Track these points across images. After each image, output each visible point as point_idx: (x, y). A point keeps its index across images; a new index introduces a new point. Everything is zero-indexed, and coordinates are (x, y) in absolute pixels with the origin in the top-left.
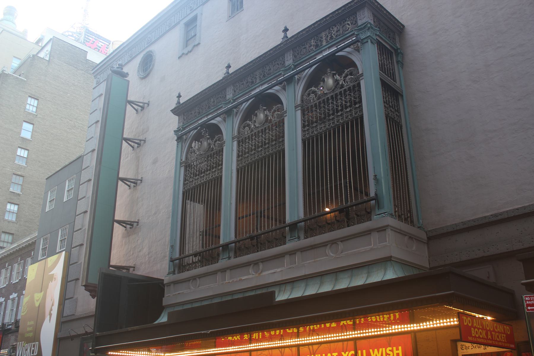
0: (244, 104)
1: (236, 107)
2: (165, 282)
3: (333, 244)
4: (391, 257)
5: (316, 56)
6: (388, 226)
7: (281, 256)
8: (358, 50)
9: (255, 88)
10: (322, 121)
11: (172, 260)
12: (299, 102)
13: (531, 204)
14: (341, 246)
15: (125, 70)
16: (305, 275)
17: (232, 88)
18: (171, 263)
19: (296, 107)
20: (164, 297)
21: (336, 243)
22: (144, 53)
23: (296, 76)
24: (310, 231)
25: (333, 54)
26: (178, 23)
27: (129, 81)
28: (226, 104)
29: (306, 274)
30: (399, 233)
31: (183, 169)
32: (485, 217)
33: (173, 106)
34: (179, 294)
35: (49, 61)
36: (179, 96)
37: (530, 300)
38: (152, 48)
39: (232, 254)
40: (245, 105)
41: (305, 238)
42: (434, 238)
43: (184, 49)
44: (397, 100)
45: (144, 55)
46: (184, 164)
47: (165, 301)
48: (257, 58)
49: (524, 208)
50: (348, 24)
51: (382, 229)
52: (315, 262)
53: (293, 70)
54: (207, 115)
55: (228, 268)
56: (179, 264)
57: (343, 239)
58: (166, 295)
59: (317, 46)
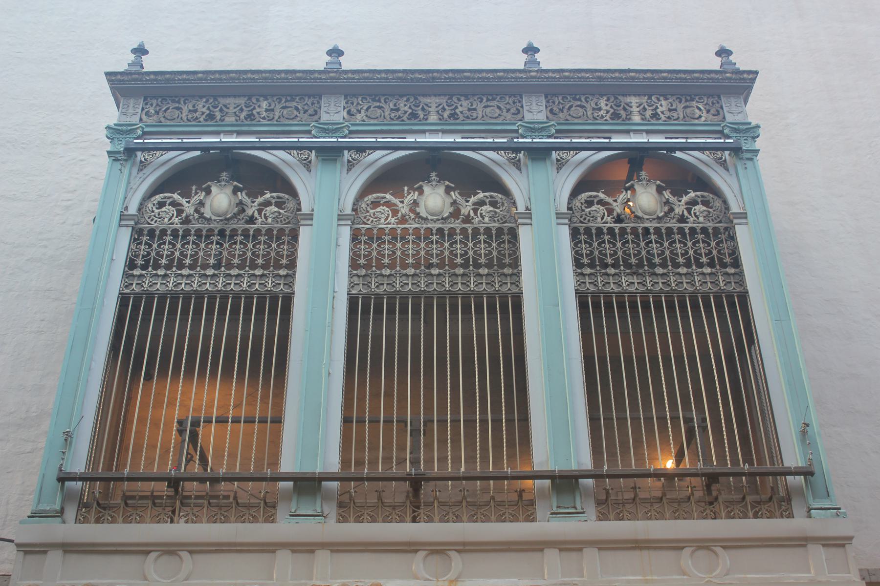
0: (379, 153)
1: (361, 149)
3: (700, 548)
5: (612, 135)
8: (723, 164)
9: (423, 132)
10: (635, 269)
11: (63, 479)
14: (726, 558)
17: (343, 103)
21: (707, 548)
25: (672, 149)
36: (140, 51)
40: (382, 158)
48: (446, 71)
50: (700, 109)
52: (647, 581)
53: (549, 137)
55: (323, 545)
57: (732, 544)
59: (615, 116)
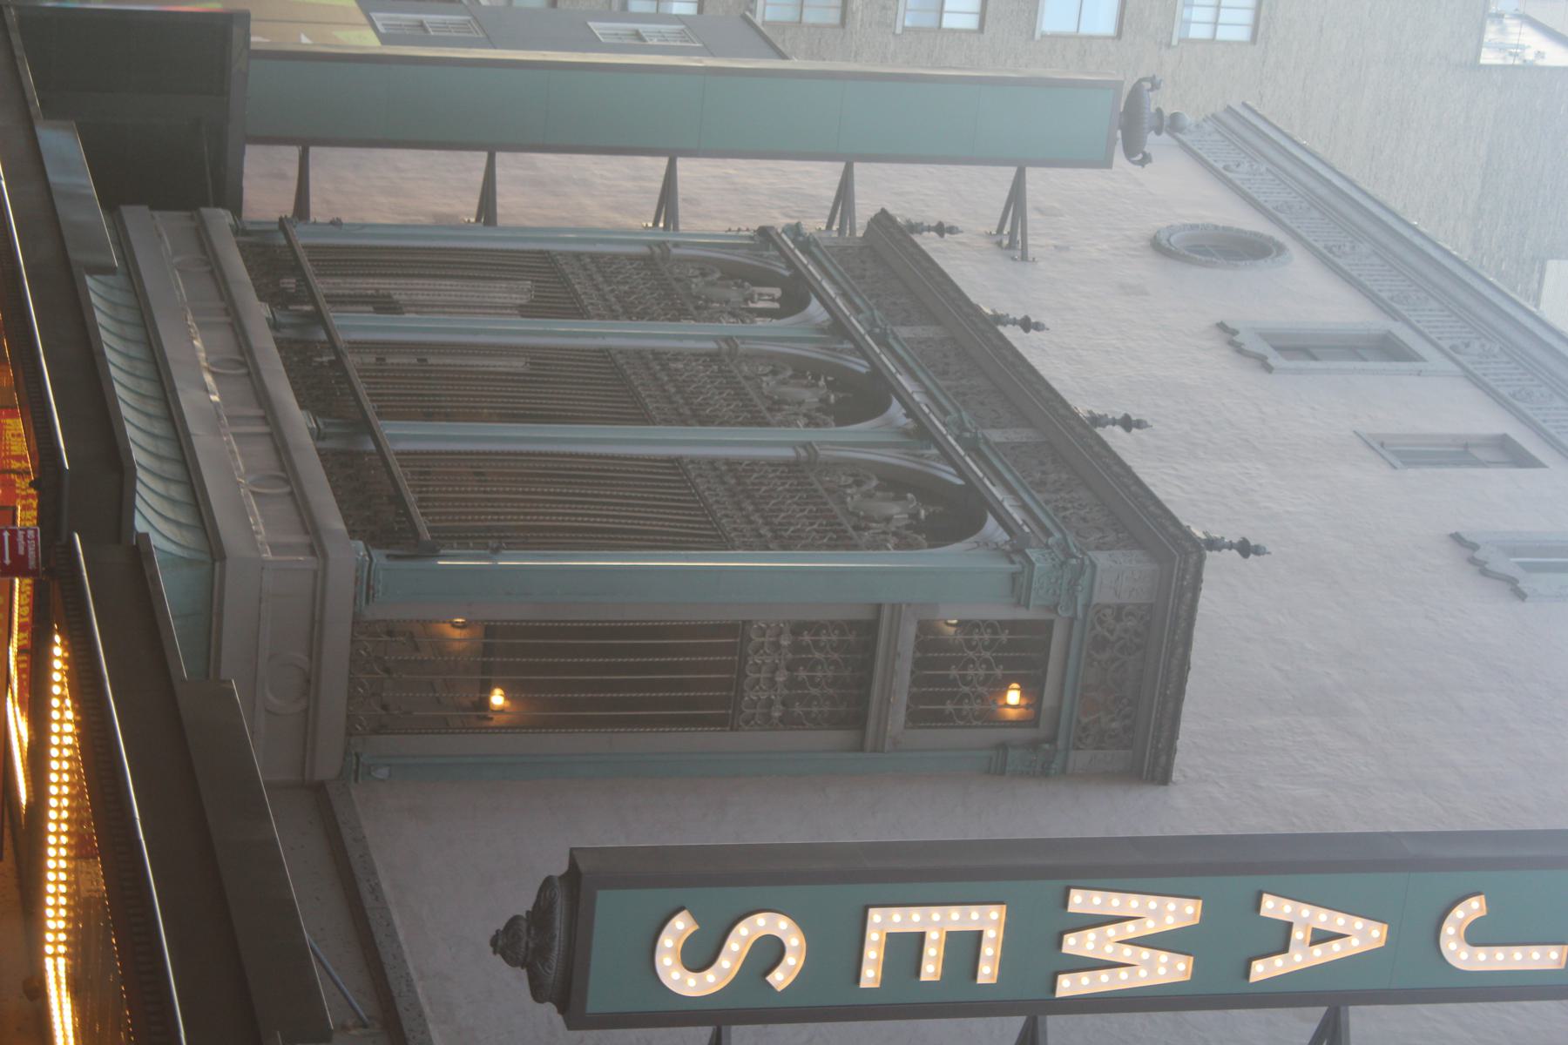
2: (204, 210)
4: (223, 558)
6: (325, 556)
7: (262, 397)
12: (825, 453)
13: (405, 947)
15: (1154, 142)
16: (188, 435)
18: (276, 227)
19: (807, 445)
20: (152, 208)
22: (1280, 236)
23: (934, 451)
24: (341, 465)
26: (1395, 315)
27: (1107, 163)
28: (872, 323)
29: (194, 439)
30: (313, 615)
31: (644, 250)
32: (374, 873)
33: (901, 213)
34: (160, 236)
35: (1476, 66)
37: (26, 538)
38: (1293, 248)
39: (288, 333)
41: (319, 451)
42: (322, 803)
43: (1266, 336)
44: (836, 722)
45: (1271, 239)
46: (657, 250)
47: (136, 217)
49: (393, 935)
51: (316, 547)
54: (845, 295)
56: (278, 260)
58: (157, 214)
